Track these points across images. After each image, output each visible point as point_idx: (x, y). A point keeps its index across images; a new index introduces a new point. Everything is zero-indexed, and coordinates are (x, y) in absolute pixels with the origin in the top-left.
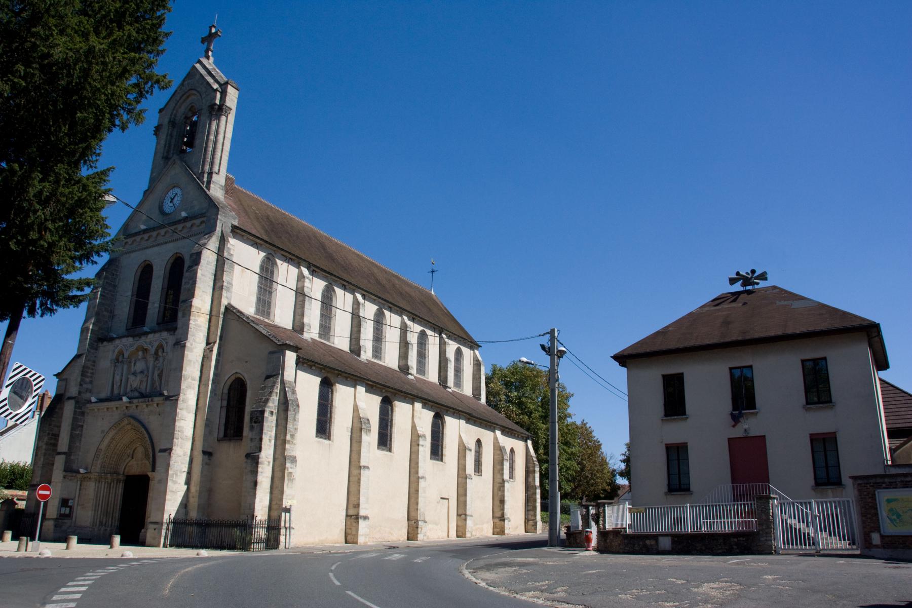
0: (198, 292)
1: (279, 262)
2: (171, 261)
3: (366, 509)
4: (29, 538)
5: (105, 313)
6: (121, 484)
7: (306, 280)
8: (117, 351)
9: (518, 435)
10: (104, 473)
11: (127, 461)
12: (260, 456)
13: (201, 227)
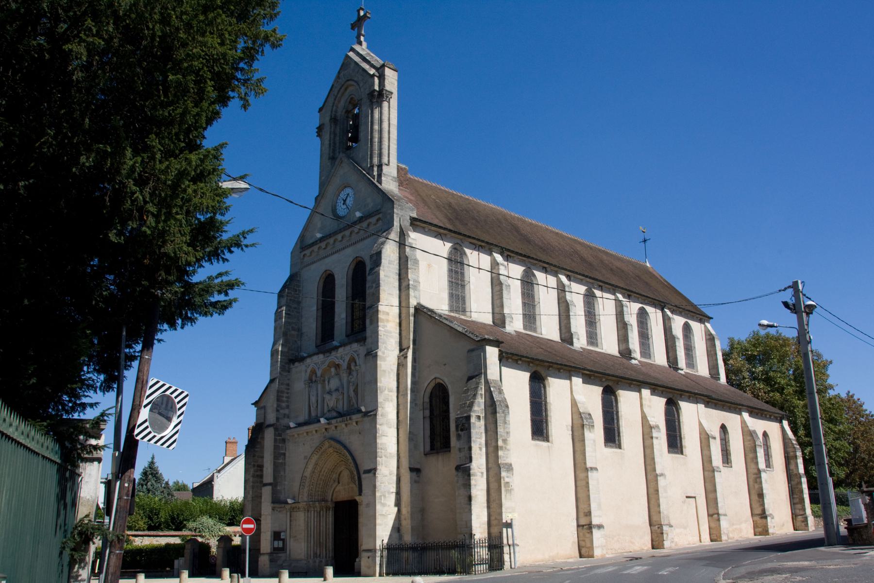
0: (383, 296)
1: (468, 251)
2: (352, 267)
3: (600, 516)
4: (240, 575)
5: (293, 332)
6: (331, 512)
7: (501, 267)
8: (309, 371)
9: (770, 416)
10: (312, 501)
11: (334, 485)
12: (471, 467)
13: (378, 225)
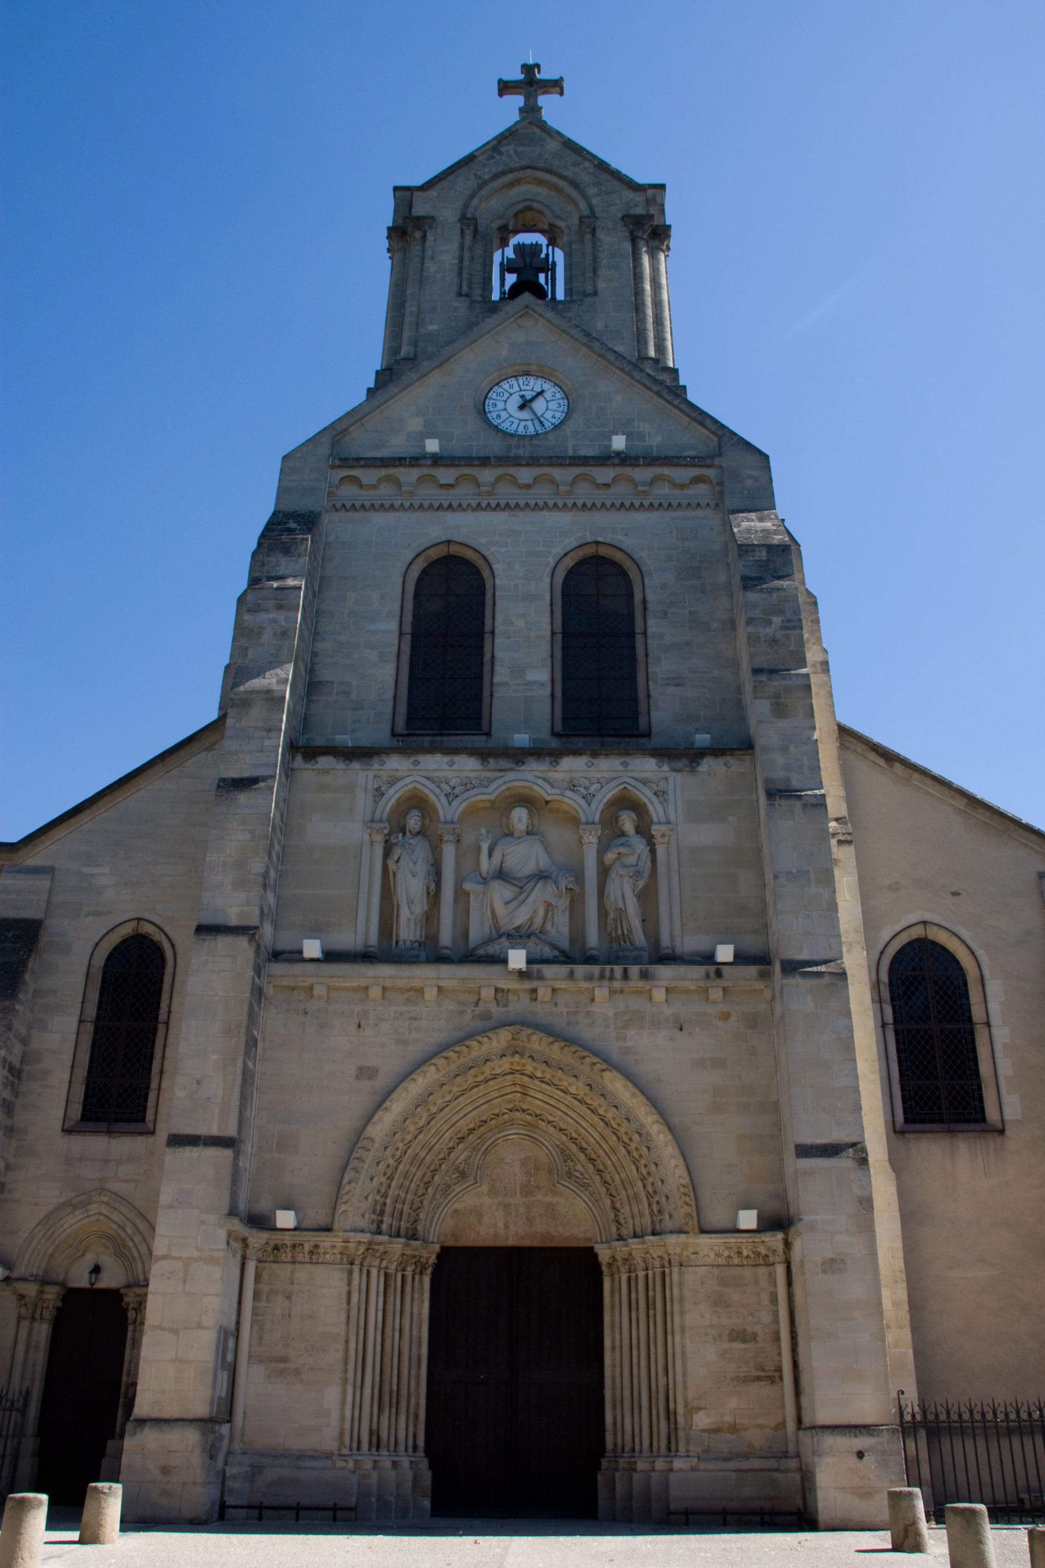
2: (569, 562)
13: (686, 491)
